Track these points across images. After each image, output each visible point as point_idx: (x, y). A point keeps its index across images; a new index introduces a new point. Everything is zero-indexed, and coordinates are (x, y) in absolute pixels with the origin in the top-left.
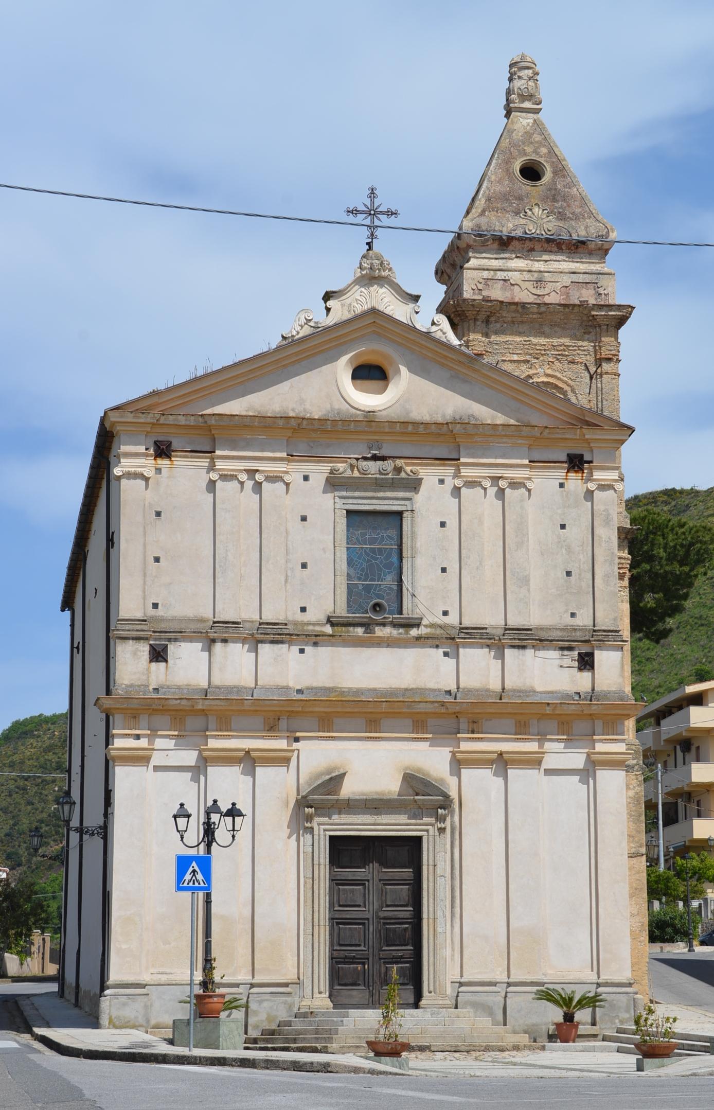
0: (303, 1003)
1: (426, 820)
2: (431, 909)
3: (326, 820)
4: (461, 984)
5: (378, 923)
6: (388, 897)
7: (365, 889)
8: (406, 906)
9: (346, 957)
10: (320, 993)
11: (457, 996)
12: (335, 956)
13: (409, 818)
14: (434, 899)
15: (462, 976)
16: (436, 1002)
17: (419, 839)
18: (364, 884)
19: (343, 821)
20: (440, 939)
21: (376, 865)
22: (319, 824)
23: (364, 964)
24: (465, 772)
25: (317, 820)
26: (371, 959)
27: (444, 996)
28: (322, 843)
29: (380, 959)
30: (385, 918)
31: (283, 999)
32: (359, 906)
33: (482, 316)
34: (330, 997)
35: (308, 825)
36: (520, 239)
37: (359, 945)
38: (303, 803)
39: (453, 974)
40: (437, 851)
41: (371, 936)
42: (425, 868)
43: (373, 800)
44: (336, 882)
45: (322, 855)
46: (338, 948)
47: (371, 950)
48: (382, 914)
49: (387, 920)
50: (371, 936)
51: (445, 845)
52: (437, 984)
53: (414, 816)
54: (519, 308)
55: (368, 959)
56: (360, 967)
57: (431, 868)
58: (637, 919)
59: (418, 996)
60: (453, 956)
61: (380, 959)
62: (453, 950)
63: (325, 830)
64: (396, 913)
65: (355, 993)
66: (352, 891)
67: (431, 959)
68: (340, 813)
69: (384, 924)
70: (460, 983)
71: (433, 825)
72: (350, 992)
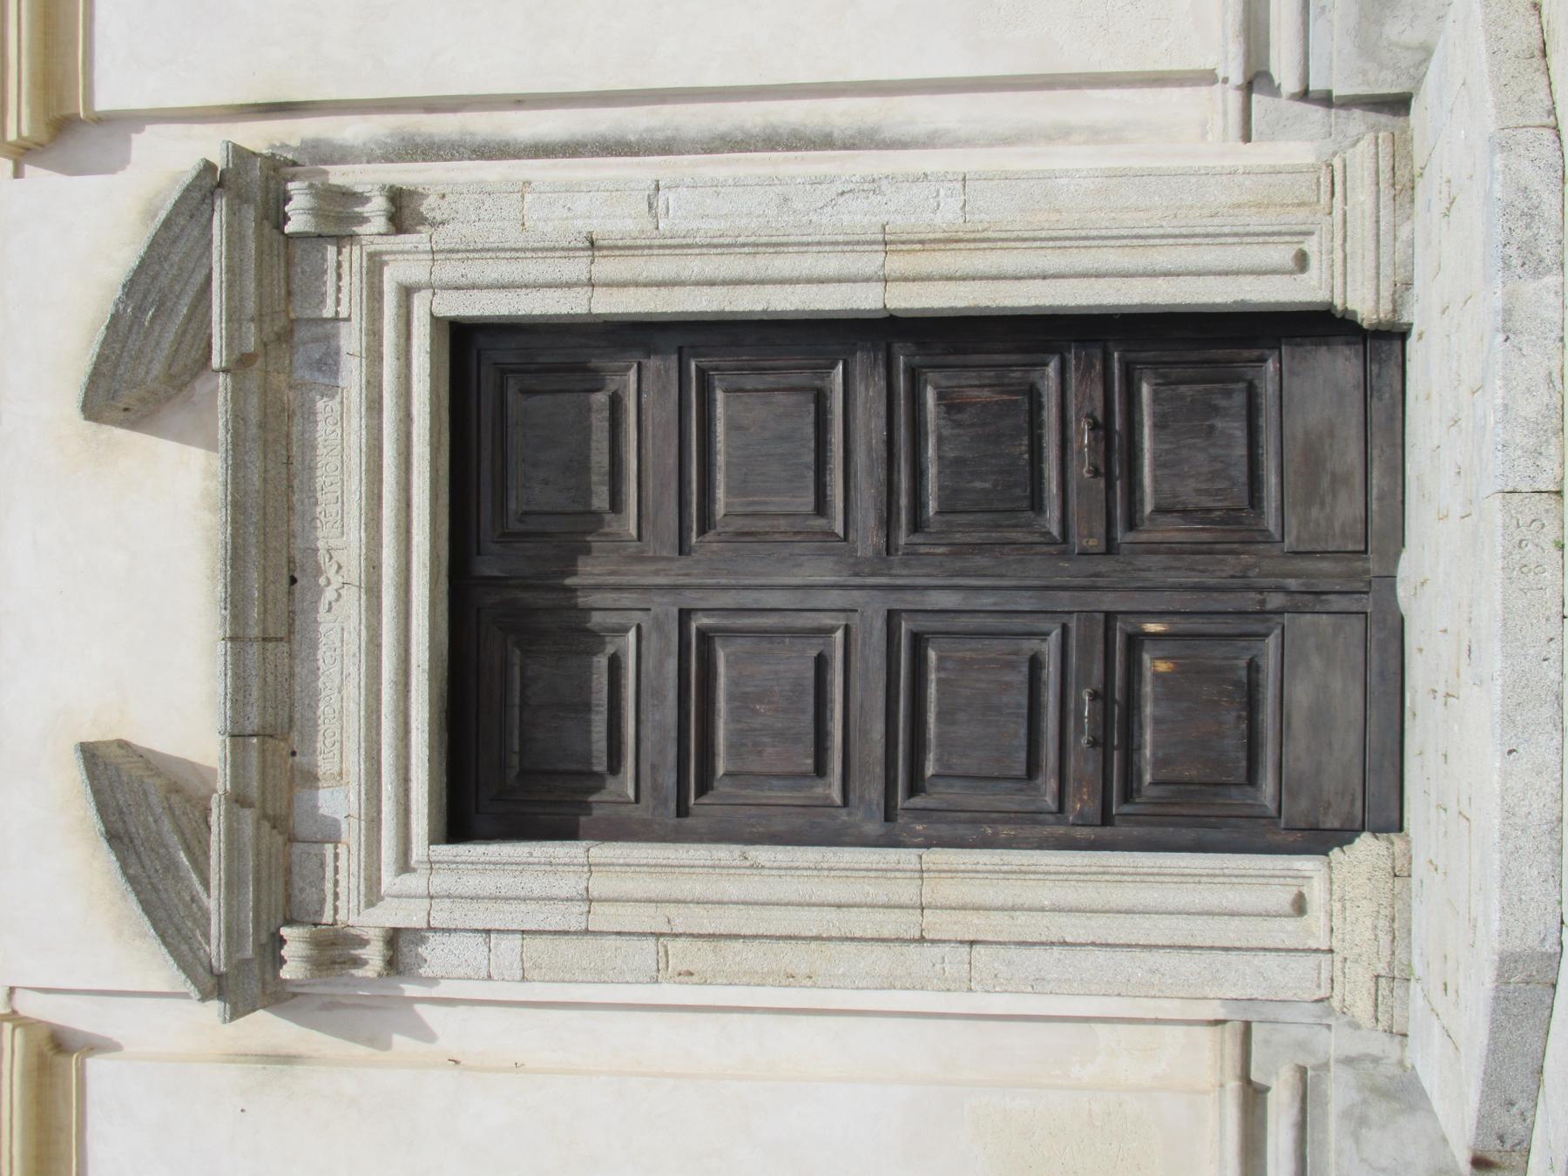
0: (1362, 1008)
1: (341, 292)
2: (831, 264)
3: (344, 867)
4: (1256, 80)
5: (912, 553)
6: (777, 503)
7: (730, 633)
8: (821, 399)
9: (1101, 743)
10: (1300, 906)
11: (1326, 100)
12: (1094, 808)
13: (331, 390)
14: (777, 247)
15: (1208, 78)
16: (1361, 230)
17: (464, 342)
18: (705, 637)
19: (354, 764)
20: (996, 210)
21: (589, 571)
22: (373, 895)
23: (1135, 642)
24: (113, 89)
25: (347, 910)
26: (1109, 602)
27: (1332, 180)
28: (472, 883)
29: (1110, 548)
30: (888, 522)
31: (1332, 1131)
32: (821, 663)
34: (1320, 838)
35: (374, 955)
37: (1035, 664)
38: (243, 983)
39: (1197, 126)
40: (514, 238)
41: (986, 601)
42: (610, 304)
43: (236, 603)
44: (696, 798)
45: (537, 884)
46: (1052, 784)
47: (1064, 601)
48: (868, 538)
49: (902, 512)
50: (986, 601)
51: (485, 191)
52: (1255, 222)
53: (328, 363)
55: (1110, 616)
56: (1154, 665)
57: (607, 268)
59: (1320, 325)
60: (1095, 134)
61: (1110, 548)
62: (1062, 134)
63: (404, 866)
64: (860, 459)
65: (1301, 694)
66: (742, 702)
67: (1113, 258)
68: (311, 778)
69: (917, 525)
70: (1248, 87)
71: (376, 264)
72: (1298, 721)
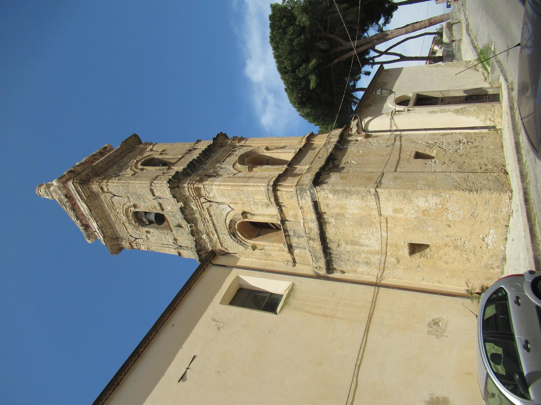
33: (116, 242)
36: (81, 222)
54: (103, 229)
58: (430, 198)
